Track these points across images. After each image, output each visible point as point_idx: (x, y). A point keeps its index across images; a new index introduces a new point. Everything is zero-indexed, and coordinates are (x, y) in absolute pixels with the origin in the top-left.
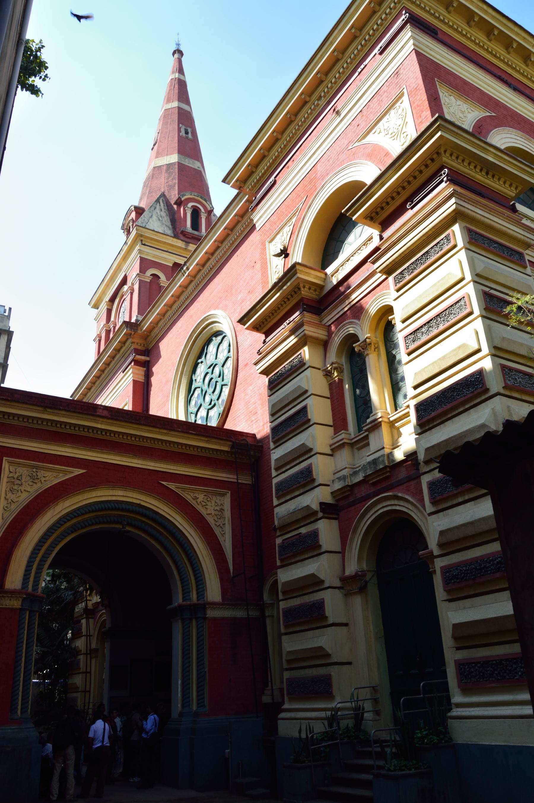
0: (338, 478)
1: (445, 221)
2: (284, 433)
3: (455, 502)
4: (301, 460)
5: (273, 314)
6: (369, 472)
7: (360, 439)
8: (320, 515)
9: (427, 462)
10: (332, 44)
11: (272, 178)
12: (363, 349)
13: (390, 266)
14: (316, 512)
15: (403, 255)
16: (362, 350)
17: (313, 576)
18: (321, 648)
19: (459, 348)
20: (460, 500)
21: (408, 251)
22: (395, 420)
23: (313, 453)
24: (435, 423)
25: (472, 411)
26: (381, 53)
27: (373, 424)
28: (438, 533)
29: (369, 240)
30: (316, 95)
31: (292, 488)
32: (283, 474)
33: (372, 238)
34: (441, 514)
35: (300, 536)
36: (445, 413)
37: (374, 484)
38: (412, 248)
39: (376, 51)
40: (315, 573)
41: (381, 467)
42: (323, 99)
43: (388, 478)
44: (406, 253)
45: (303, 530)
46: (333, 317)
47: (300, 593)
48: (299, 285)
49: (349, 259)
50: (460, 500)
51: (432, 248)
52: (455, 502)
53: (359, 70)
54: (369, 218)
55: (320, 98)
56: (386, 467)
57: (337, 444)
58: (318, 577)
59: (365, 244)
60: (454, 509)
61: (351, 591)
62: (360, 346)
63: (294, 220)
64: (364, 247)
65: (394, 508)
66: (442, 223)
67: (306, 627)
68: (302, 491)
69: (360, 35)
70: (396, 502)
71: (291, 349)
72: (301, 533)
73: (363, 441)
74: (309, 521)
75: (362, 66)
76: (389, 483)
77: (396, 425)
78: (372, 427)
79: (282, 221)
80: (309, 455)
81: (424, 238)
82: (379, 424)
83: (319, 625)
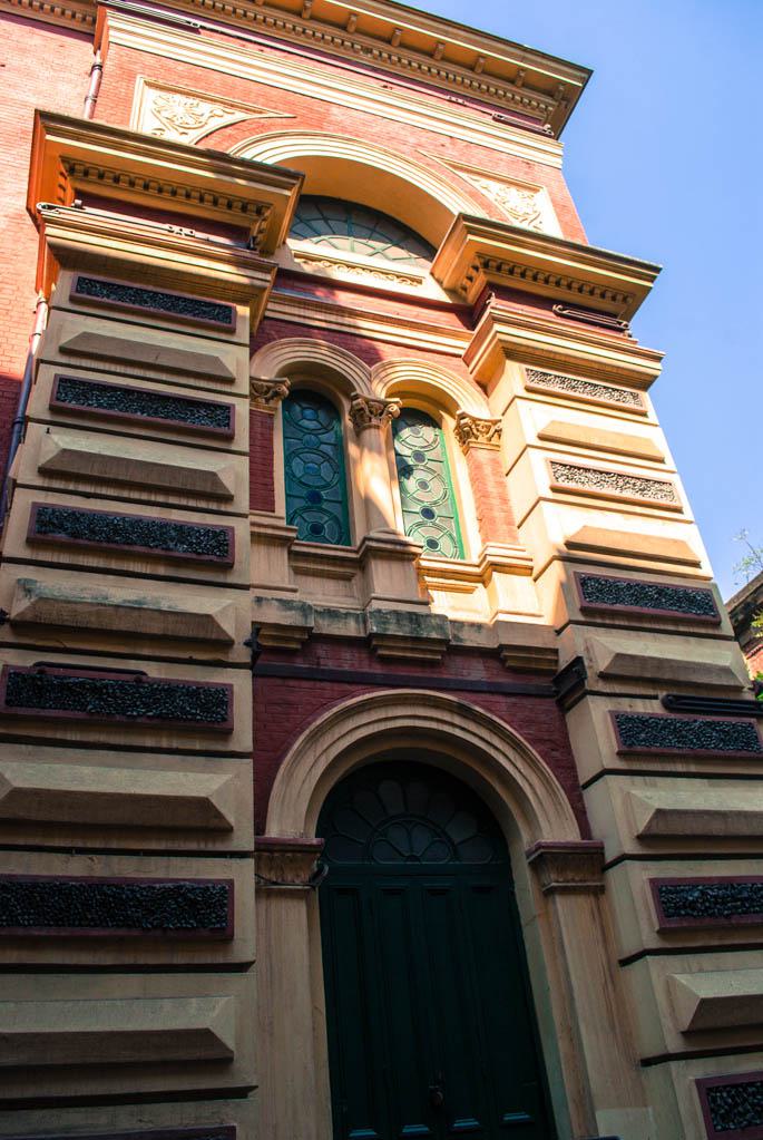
0: (280, 600)
1: (636, 375)
2: (114, 412)
3: (669, 767)
4: (192, 503)
5: (146, 187)
6: (392, 630)
7: (315, 555)
8: (241, 654)
9: (604, 676)
10: (446, 34)
11: (200, 23)
12: (371, 412)
13: (523, 349)
14: (227, 644)
15: (552, 356)
16: (367, 411)
17: (203, 805)
18: (206, 1036)
19: (675, 541)
20: (680, 768)
21: (563, 358)
22: (429, 569)
23: (230, 509)
24: (617, 622)
25: (692, 639)
26: (494, 119)
27: (398, 547)
28: (653, 811)
29: (413, 280)
30: (368, 42)
31: (126, 548)
32: (79, 498)
33: (420, 282)
34: (638, 779)
35: (139, 681)
36: (640, 617)
37: (385, 660)
38: (572, 360)
39: (493, 113)
40: (214, 801)
41: (434, 635)
42: (369, 55)
43: (432, 664)
44: (558, 357)
45: (154, 671)
46: (285, 313)
47: (80, 844)
48: (269, 208)
49: (354, 267)
50: (680, 768)
51: (605, 387)
52: (669, 767)
53: (454, 99)
54: (482, 260)
55: (368, 51)
56: (445, 642)
57: (270, 531)
58: (219, 815)
59: (401, 277)
60: (669, 780)
61: (276, 883)
62: (367, 403)
63: (239, 116)
64: (409, 282)
65: (446, 728)
66: (631, 374)
67: (107, 959)
68: (162, 571)
69: (478, 74)
70: (457, 720)
71: (197, 280)
72: (144, 674)
73: (321, 563)
74: (185, 655)
75: (460, 101)
76: (435, 676)
77: (427, 579)
78: (391, 551)
79: (197, 88)
80: (213, 506)
81: (596, 366)
82: (411, 556)
83: (179, 959)
